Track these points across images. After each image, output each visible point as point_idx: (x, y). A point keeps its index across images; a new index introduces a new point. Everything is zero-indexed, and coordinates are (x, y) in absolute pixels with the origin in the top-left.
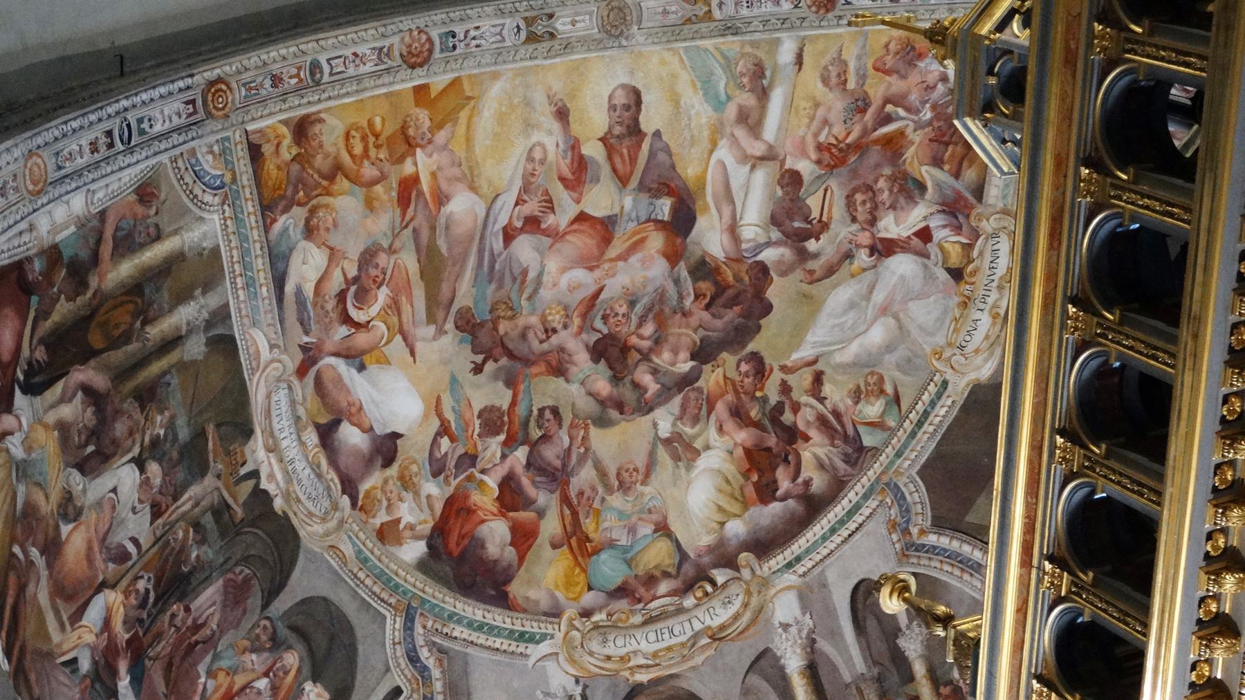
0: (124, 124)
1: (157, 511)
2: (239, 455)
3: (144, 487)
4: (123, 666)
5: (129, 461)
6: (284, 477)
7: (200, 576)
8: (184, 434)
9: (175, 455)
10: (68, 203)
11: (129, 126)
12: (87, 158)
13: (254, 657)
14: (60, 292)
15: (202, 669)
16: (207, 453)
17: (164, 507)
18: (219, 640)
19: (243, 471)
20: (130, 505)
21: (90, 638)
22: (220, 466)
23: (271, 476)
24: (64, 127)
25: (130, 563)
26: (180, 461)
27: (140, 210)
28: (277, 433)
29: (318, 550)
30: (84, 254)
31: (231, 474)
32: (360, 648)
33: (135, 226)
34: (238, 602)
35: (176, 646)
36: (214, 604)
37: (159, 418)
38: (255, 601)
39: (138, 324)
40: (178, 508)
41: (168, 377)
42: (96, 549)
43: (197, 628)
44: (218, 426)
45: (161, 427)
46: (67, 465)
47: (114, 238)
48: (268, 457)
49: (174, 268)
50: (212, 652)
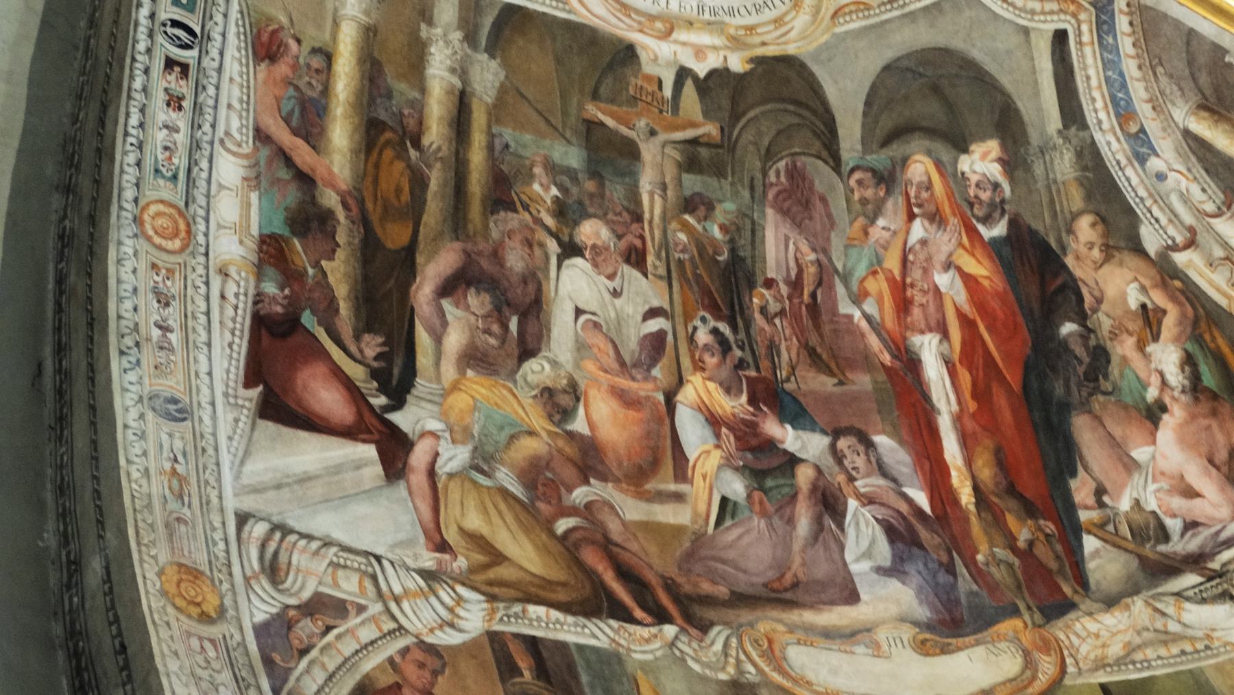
0: (170, 30)
1: (636, 258)
2: (645, 85)
3: (600, 259)
4: (772, 428)
5: (559, 267)
6: (711, 32)
7: (744, 241)
8: (572, 156)
9: (590, 186)
10: (221, 187)
11: (176, 24)
12: (181, 121)
13: (881, 222)
14: (317, 265)
15: (846, 307)
16: (616, 133)
17: (638, 243)
18: (830, 259)
19: (668, 92)
20: (607, 296)
21: (716, 457)
22: (642, 123)
23: (699, 52)
24: (131, 140)
25: (670, 338)
26: (602, 185)
27: (282, 69)
28: (654, 10)
29: (825, 38)
30: (292, 195)
31: (661, 112)
32: (977, 54)
33: (297, 88)
34: (807, 202)
35: (800, 332)
36: (787, 239)
37: (536, 187)
38: (820, 174)
39: (413, 154)
40: (651, 222)
41: (497, 141)
42: (624, 383)
43: (796, 285)
44: (595, 96)
45: (546, 189)
46: (512, 375)
47: (295, 132)
48: (676, 42)
49: (376, 54)
50: (837, 280)
